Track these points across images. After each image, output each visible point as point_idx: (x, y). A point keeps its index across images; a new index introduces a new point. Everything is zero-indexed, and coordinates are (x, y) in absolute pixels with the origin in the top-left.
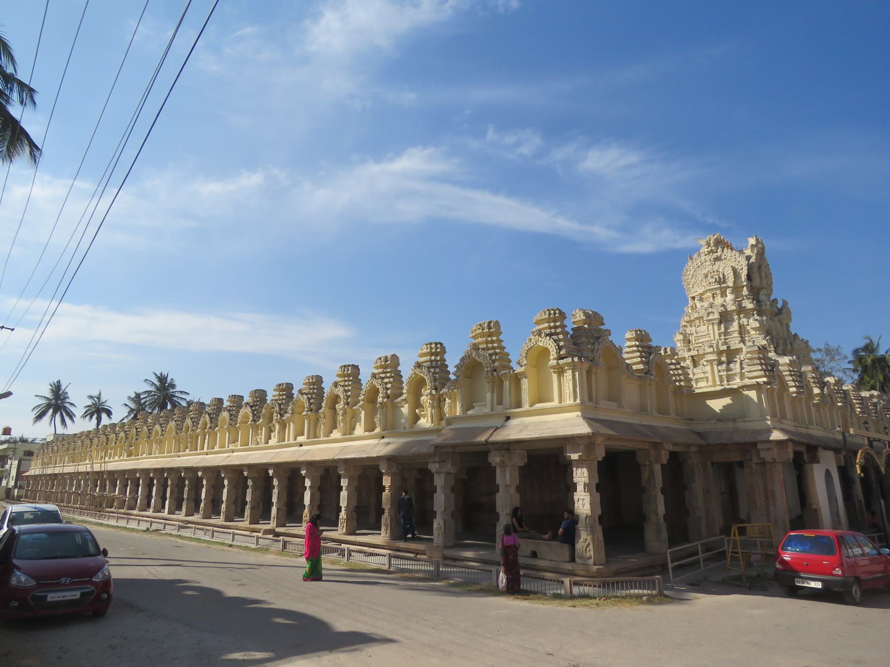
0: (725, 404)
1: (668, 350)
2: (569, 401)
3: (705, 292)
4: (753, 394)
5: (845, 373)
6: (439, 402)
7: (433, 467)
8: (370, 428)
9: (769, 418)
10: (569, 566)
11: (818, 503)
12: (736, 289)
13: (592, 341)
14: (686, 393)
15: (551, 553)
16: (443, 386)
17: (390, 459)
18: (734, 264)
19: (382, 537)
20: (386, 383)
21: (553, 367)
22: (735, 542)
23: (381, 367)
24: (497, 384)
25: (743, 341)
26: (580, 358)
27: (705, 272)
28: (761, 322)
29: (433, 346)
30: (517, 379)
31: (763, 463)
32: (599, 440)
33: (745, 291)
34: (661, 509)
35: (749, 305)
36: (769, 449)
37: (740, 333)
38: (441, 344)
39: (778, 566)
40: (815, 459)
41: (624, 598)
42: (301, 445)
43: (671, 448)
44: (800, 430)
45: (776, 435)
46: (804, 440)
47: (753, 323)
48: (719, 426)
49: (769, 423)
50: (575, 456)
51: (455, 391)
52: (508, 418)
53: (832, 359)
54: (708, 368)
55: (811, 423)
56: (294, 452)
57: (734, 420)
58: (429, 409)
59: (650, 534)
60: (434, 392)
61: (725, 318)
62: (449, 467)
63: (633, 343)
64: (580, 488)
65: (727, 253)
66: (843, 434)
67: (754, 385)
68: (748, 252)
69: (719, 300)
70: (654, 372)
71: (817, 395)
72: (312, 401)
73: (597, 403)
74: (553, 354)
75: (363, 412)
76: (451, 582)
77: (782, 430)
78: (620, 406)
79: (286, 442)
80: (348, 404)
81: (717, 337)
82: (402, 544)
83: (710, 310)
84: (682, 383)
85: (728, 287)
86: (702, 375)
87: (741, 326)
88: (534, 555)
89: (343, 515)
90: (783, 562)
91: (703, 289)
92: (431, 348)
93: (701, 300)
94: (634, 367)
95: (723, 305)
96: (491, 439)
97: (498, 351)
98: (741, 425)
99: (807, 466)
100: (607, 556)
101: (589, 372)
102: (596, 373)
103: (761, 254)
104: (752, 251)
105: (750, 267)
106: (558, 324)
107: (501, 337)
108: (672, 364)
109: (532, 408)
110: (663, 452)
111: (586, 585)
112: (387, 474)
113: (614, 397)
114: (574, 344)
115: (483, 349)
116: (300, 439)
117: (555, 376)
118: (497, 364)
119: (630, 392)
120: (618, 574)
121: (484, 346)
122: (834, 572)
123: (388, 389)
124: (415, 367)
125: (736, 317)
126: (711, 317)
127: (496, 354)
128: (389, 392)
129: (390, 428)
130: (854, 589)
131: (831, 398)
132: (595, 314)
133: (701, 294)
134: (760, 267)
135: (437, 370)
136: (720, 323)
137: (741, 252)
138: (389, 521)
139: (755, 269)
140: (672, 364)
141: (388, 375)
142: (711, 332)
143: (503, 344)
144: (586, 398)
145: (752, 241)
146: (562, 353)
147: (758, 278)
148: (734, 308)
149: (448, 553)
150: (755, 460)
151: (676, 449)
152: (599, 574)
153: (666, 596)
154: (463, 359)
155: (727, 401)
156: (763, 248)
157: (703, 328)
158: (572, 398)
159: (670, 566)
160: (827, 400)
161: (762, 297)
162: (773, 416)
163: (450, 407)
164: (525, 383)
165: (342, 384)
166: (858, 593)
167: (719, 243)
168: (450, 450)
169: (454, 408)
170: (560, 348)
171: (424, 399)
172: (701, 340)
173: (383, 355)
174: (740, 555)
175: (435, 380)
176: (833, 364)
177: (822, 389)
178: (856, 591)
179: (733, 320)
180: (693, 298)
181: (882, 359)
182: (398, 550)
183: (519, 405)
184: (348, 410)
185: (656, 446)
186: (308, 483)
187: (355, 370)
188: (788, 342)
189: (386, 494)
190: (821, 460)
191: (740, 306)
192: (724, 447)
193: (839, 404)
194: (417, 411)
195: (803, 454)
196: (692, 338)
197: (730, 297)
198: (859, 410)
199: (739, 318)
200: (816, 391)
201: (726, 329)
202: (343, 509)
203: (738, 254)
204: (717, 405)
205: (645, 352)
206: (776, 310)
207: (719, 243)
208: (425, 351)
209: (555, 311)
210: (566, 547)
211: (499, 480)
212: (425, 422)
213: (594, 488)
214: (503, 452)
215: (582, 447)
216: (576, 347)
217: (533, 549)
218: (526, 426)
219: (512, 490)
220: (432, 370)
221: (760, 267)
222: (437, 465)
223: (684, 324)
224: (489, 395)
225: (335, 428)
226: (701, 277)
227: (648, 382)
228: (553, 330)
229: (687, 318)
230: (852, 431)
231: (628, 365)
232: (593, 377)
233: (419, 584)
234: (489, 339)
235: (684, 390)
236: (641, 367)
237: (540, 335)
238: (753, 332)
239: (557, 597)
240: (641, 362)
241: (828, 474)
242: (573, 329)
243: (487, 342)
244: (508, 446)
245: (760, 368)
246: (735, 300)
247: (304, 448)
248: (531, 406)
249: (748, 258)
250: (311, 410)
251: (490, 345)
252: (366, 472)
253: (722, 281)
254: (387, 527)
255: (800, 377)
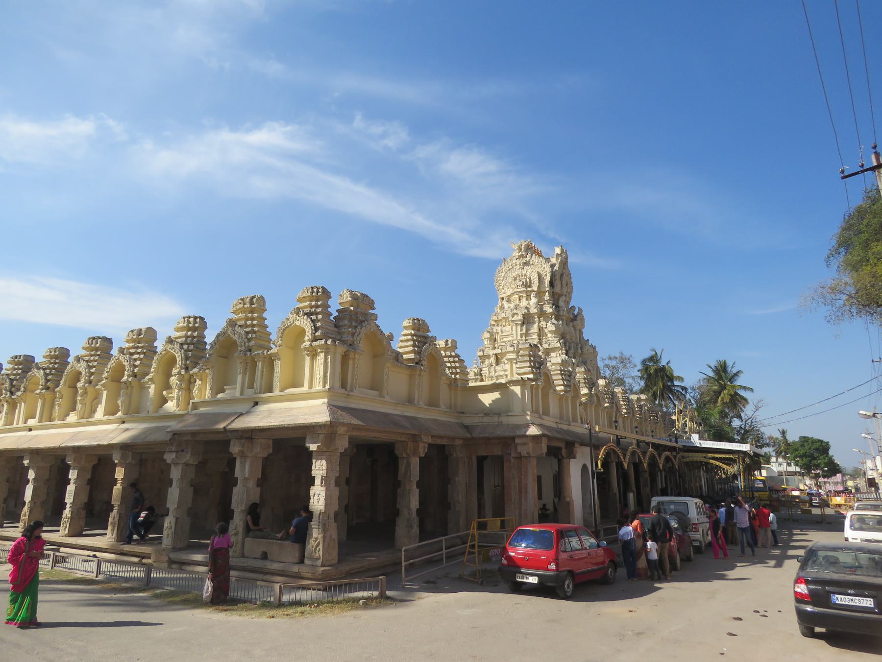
0: (494, 398)
1: (449, 342)
2: (318, 387)
3: (513, 294)
4: (517, 389)
5: (634, 379)
6: (188, 384)
7: (169, 457)
8: (111, 411)
9: (528, 413)
10: (296, 569)
11: (571, 497)
12: (540, 294)
13: (354, 324)
14: (459, 386)
15: (284, 554)
16: (196, 364)
17: (124, 447)
18: (539, 270)
19: (106, 539)
20: (135, 360)
21: (306, 349)
22: (473, 536)
23: (133, 340)
24: (251, 365)
25: (541, 343)
26: (334, 341)
27: (515, 275)
28: (557, 326)
29: (191, 320)
30: (270, 361)
31: (520, 457)
32: (341, 430)
33: (547, 297)
34: (414, 502)
35: (548, 309)
36: (524, 444)
37: (539, 335)
38: (202, 319)
39: (505, 562)
40: (572, 455)
41: (339, 602)
42: (30, 430)
43: (430, 441)
44: (560, 426)
45: (533, 431)
46: (559, 436)
47: (550, 327)
48: (487, 419)
49: (528, 418)
50: (313, 447)
51: (207, 371)
52: (256, 404)
53: (625, 367)
54: (508, 367)
55: (575, 420)
56: (20, 437)
57: (499, 415)
58: (176, 391)
59: (400, 530)
60: (183, 372)
61: (527, 320)
62: (187, 457)
63: (408, 332)
64: (318, 481)
65: (535, 259)
66: (590, 430)
67: (518, 381)
68: (553, 260)
69: (524, 303)
70: (424, 363)
71: (585, 395)
72: (50, 377)
73: (352, 390)
74: (308, 335)
75: (105, 393)
76: (159, 591)
77: (540, 426)
78: (381, 396)
79: (15, 425)
80: (90, 382)
81: (519, 338)
82: (127, 548)
83: (515, 311)
84: (458, 376)
85: (533, 291)
86: (502, 373)
87: (540, 329)
88: (265, 556)
89: (67, 513)
90: (510, 558)
91: (511, 291)
92: (189, 322)
93: (509, 301)
94: (405, 357)
95: (527, 308)
96: (229, 427)
97: (256, 329)
98: (505, 420)
99: (565, 461)
100: (339, 555)
101: (345, 358)
102: (354, 359)
103: (564, 263)
104: (557, 259)
105: (553, 274)
106: (319, 303)
107: (264, 315)
108: (446, 356)
109: (282, 393)
110: (421, 445)
111: (314, 589)
112: (121, 465)
113: (376, 385)
114: (336, 326)
115: (241, 326)
116: (32, 422)
117: (308, 359)
118: (252, 343)
119: (396, 381)
120: (350, 574)
121: (242, 323)
122: (549, 567)
123: (136, 366)
124: (167, 342)
125: (537, 320)
126: (515, 318)
127: (254, 332)
128: (136, 370)
129: (133, 412)
130: (566, 583)
131: (598, 398)
132: (365, 296)
133: (509, 296)
134: (562, 275)
135: (192, 347)
136: (523, 324)
137: (548, 260)
138: (117, 519)
139: (558, 277)
140: (446, 356)
141: (139, 350)
142: (514, 332)
143: (266, 322)
144: (338, 384)
145: (558, 250)
146: (317, 334)
147: (559, 284)
148: (535, 311)
149: (173, 556)
150: (513, 455)
151: (439, 442)
152: (325, 577)
153: (388, 598)
154: (218, 336)
155: (496, 395)
156: (566, 259)
157: (508, 328)
158: (321, 384)
159: (404, 564)
160: (595, 399)
161: (561, 303)
162: (534, 411)
163: (200, 390)
164: (278, 364)
165: (87, 358)
166: (571, 586)
167: (529, 249)
168: (189, 438)
169: (203, 391)
170: (316, 329)
171: (174, 380)
172: (505, 340)
173: (137, 327)
174: (476, 550)
175: (187, 358)
176: (625, 371)
177: (590, 389)
178: (568, 585)
179: (534, 323)
180: (503, 299)
181: (663, 369)
182: (123, 554)
183: (270, 390)
184: (90, 389)
185: (415, 438)
186: (31, 475)
187: (105, 343)
188: (579, 346)
189: (117, 488)
190: (577, 456)
191: (541, 309)
192: (488, 441)
193: (606, 405)
194: (164, 393)
195: (559, 448)
196: (498, 337)
197: (534, 300)
198: (625, 411)
199: (540, 321)
200: (584, 391)
201: (527, 330)
202: (68, 506)
203: (544, 261)
204: (487, 399)
205: (419, 342)
206: (572, 316)
207: (529, 249)
208: (181, 325)
209: (312, 288)
210: (297, 546)
211: (238, 473)
212: (171, 406)
213: (333, 482)
214: (243, 441)
215: (322, 437)
216: (336, 329)
217: (264, 550)
218: (271, 412)
219: (252, 484)
220: (185, 347)
221: (562, 275)
222: (174, 455)
223: (493, 323)
224: (239, 378)
225: (74, 409)
226: (510, 279)
227: (418, 372)
228: (313, 310)
229: (495, 318)
230: (597, 429)
231: (398, 353)
232: (351, 362)
233: (118, 596)
234: (249, 315)
235: (459, 384)
236: (412, 356)
237: (298, 314)
238: (550, 335)
239: (267, 605)
240: (413, 352)
241: (584, 467)
242: (338, 311)
243: (247, 319)
244: (250, 435)
245: (528, 364)
246: (538, 303)
247: (33, 433)
248: (281, 391)
249: (552, 266)
250: (48, 388)
251: (249, 322)
252: (98, 461)
253: (528, 285)
254: (114, 526)
255: (568, 377)
